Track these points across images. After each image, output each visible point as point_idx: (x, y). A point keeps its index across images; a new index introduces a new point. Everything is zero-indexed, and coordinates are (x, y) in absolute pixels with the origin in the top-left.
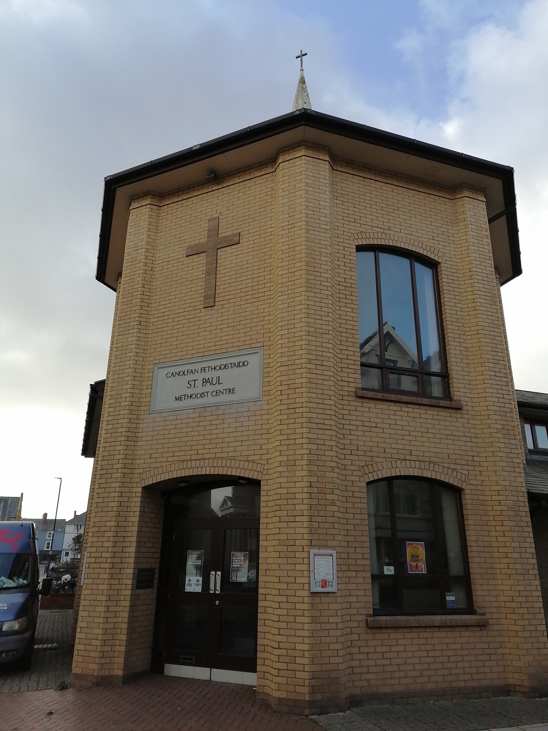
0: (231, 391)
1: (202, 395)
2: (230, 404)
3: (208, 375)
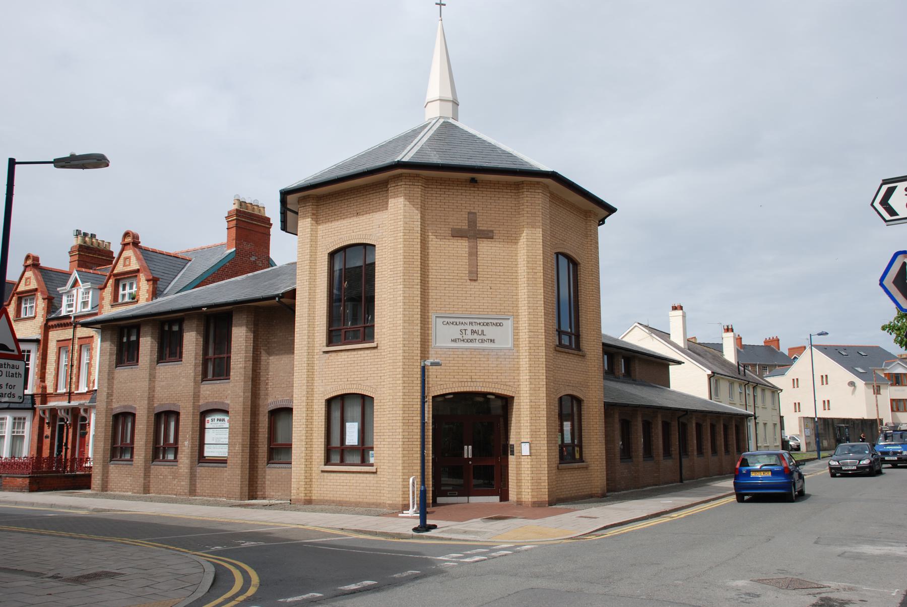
0: (492, 341)
1: (471, 341)
2: (492, 350)
3: (475, 328)
